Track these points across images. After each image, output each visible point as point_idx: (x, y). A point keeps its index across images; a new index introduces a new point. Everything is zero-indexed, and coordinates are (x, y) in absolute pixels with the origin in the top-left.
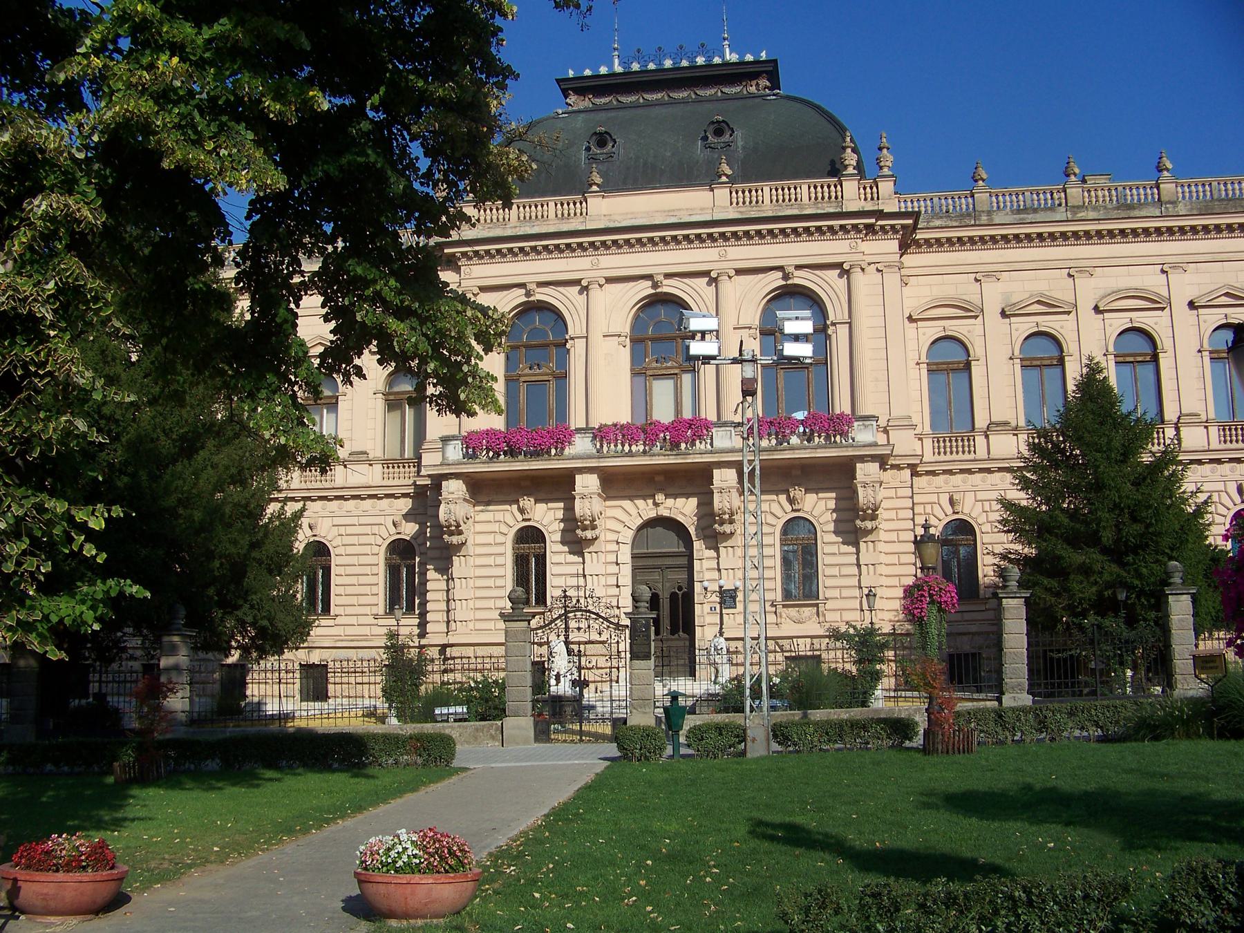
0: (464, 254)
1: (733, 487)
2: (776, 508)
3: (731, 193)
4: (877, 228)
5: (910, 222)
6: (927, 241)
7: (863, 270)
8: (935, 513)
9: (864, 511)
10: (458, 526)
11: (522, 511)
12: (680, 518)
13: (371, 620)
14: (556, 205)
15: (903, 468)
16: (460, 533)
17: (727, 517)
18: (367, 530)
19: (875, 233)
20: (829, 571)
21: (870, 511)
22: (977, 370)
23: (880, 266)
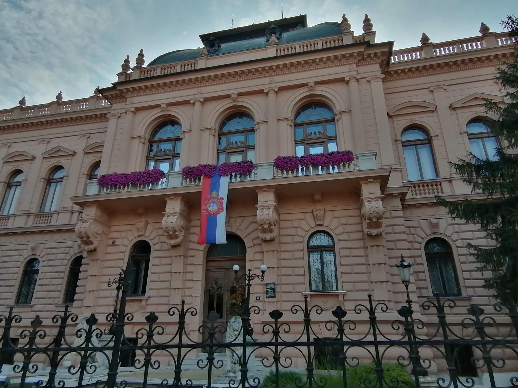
0: (128, 90)
1: (271, 205)
2: (304, 224)
3: (277, 51)
4: (366, 56)
5: (387, 50)
6: (396, 72)
7: (358, 80)
8: (419, 234)
9: (370, 219)
10: (88, 237)
11: (138, 229)
12: (239, 233)
13: (52, 307)
14: (181, 66)
15: (396, 196)
16: (92, 243)
17: (266, 226)
18: (62, 250)
19: (363, 59)
20: (345, 269)
21: (374, 220)
22: (436, 142)
23: (368, 79)
